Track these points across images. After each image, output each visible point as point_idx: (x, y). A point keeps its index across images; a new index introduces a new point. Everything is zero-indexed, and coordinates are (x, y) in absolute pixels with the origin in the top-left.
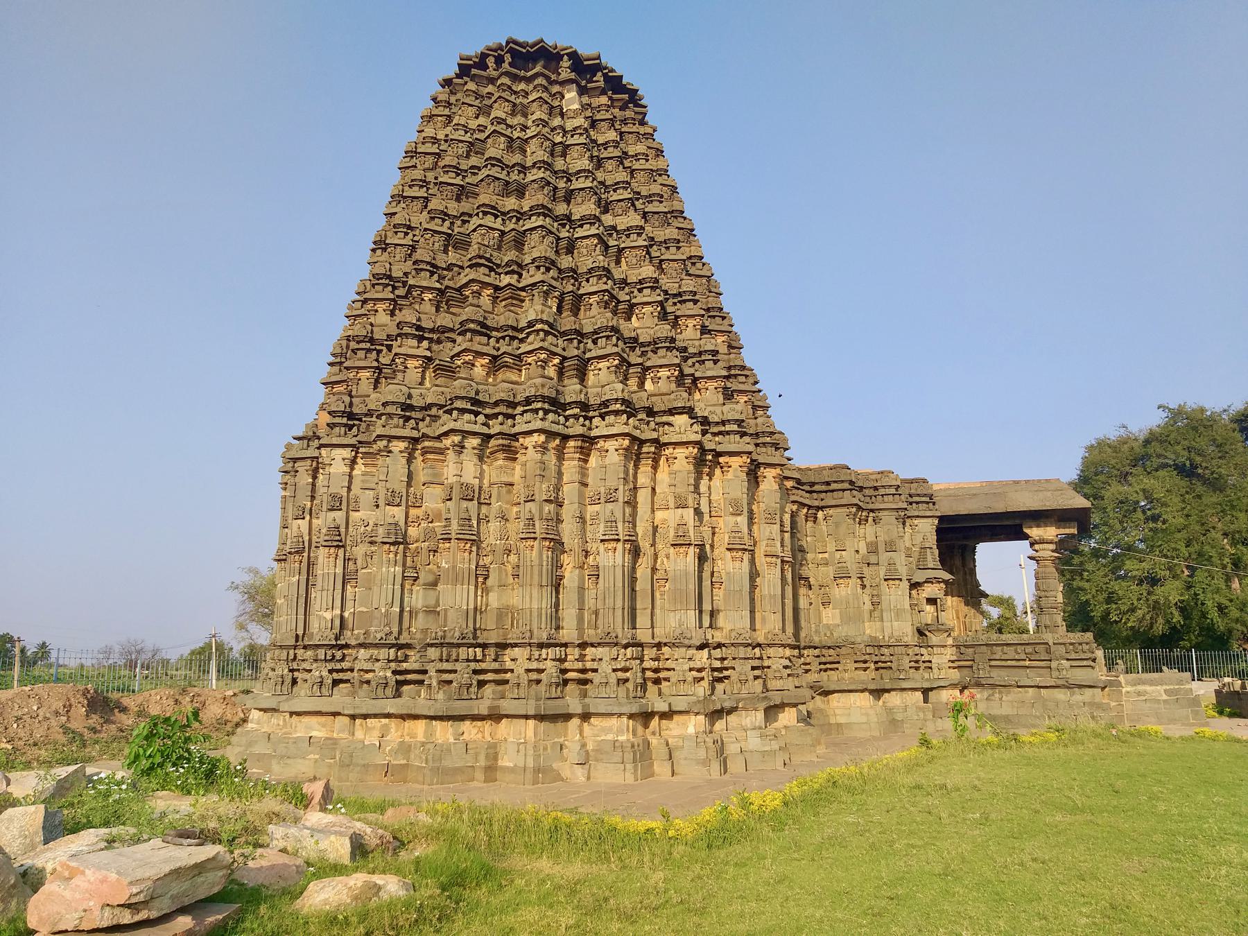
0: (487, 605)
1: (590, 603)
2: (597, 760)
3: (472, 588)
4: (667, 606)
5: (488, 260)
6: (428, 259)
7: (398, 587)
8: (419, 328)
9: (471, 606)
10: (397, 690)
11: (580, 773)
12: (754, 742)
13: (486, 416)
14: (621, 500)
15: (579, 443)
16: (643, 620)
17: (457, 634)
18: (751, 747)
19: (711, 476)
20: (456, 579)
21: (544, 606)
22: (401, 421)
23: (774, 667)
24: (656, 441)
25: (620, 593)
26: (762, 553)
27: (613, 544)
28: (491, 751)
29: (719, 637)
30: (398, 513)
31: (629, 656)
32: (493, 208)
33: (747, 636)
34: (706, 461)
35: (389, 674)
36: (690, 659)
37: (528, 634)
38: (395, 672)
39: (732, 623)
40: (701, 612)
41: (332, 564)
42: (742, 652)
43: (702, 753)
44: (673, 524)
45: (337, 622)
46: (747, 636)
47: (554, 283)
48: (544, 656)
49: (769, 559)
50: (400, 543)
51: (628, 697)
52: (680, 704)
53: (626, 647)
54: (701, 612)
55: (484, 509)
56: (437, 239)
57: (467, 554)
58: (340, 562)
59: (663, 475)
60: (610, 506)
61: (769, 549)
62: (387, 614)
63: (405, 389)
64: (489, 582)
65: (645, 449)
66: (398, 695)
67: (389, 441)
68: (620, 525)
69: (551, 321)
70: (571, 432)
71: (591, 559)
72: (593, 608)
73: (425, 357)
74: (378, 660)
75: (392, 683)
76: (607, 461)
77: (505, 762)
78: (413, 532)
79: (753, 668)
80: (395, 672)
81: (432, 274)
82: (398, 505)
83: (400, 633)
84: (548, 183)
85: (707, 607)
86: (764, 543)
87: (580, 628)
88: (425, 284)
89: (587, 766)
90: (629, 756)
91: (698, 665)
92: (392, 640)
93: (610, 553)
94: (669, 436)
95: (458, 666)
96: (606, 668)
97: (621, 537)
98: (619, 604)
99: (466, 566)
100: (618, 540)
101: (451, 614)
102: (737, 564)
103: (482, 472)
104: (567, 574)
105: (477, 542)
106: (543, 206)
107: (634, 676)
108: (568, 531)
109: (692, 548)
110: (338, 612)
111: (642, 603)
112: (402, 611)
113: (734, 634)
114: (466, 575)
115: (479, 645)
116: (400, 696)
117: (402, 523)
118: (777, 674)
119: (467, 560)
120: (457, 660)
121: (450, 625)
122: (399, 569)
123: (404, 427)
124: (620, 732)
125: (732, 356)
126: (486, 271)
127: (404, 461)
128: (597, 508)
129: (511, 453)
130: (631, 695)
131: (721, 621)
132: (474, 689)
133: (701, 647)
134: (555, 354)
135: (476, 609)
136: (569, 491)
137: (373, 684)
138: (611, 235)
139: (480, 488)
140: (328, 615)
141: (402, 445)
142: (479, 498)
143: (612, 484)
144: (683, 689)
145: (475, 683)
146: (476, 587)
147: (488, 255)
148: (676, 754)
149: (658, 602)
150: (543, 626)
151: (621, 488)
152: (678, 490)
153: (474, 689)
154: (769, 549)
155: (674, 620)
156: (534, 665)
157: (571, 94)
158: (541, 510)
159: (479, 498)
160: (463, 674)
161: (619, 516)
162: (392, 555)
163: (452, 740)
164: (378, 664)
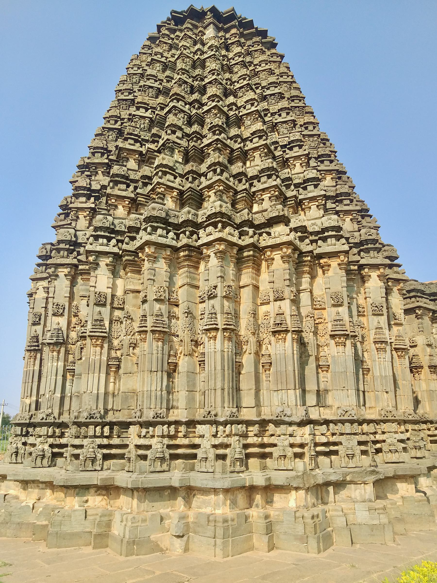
0: (119, 390)
1: (200, 386)
2: (195, 532)
3: (103, 376)
4: (273, 387)
5: (136, 135)
6: (101, 145)
7: (60, 378)
8: (89, 189)
9: (102, 390)
10: (52, 461)
11: (178, 544)
12: (362, 515)
13: (118, 241)
14: (219, 295)
15: (187, 253)
16: (248, 399)
17: (85, 414)
18: (359, 521)
19: (313, 277)
20: (90, 369)
21: (153, 388)
22: (66, 253)
23: (388, 441)
24: (254, 246)
25: (219, 376)
26: (372, 340)
27: (213, 334)
28: (106, 519)
29: (327, 414)
30: (63, 322)
31: (227, 432)
32: (145, 104)
33: (353, 413)
34: (304, 263)
35: (46, 447)
36: (291, 435)
37: (138, 414)
38: (52, 446)
39: (341, 401)
40: (304, 391)
41: (32, 363)
42: (347, 428)
43: (300, 529)
44: (272, 315)
45: (33, 406)
46: (355, 414)
47: (178, 141)
48: (151, 433)
49: (378, 346)
50: (61, 344)
51: (224, 472)
52: (279, 478)
53: (225, 424)
54: (304, 391)
55: (117, 313)
56: (110, 133)
57: (98, 349)
58: (38, 362)
59: (265, 276)
60: (212, 302)
61: (378, 336)
62: (51, 399)
63: (72, 231)
64: (121, 371)
65: (245, 254)
66: (52, 464)
67: (56, 268)
68: (219, 316)
69: (171, 164)
70: (179, 245)
71: (201, 349)
72: (203, 390)
73: (90, 208)
74: (40, 436)
75: (48, 454)
76: (210, 264)
77: (117, 530)
78: (73, 335)
79: (360, 443)
80: (52, 446)
81: (103, 154)
82: (62, 315)
83: (60, 414)
84: (186, 82)
85: (311, 386)
86: (373, 332)
87: (189, 407)
88: (96, 161)
89: (185, 538)
90: (220, 532)
91: (298, 440)
92: (51, 420)
93: (212, 341)
94: (265, 241)
95: (86, 442)
96: (206, 444)
97: (219, 326)
98: (219, 385)
99: (98, 357)
100: (217, 329)
101: (86, 398)
102: (341, 348)
103: (114, 284)
104: (180, 363)
105: (107, 338)
106: (178, 95)
107: (235, 450)
108: (180, 326)
109: (289, 334)
110: (34, 398)
111: (246, 383)
112: (62, 399)
113: (340, 411)
114: (97, 365)
115: (106, 424)
116: (55, 465)
117: (64, 329)
118: (392, 448)
119: (98, 353)
120: (86, 437)
121: (84, 407)
122: (61, 364)
123: (68, 257)
124: (216, 506)
125: (338, 187)
126: (132, 142)
127: (68, 283)
128: (203, 305)
129: (136, 267)
130: (229, 469)
131: (330, 400)
132: (99, 462)
133: (302, 424)
134: (172, 188)
135: (106, 394)
136: (181, 294)
137: (34, 455)
138: (231, 109)
139: (113, 296)
140: (28, 401)
141: (66, 271)
142: (112, 303)
143: (212, 283)
144: (283, 464)
145: (99, 456)
146: (108, 374)
147: (136, 133)
148: (276, 528)
149: (264, 384)
150: (152, 406)
151: (219, 285)
152: (276, 286)
153: (99, 462)
154: (378, 336)
155: (280, 400)
156: (142, 442)
157: (210, 32)
158: (151, 308)
159: (112, 303)
160: (89, 447)
161: (218, 309)
162: (55, 354)
163: (77, 507)
164: (39, 439)
